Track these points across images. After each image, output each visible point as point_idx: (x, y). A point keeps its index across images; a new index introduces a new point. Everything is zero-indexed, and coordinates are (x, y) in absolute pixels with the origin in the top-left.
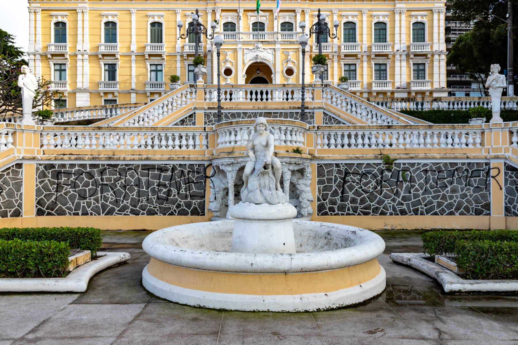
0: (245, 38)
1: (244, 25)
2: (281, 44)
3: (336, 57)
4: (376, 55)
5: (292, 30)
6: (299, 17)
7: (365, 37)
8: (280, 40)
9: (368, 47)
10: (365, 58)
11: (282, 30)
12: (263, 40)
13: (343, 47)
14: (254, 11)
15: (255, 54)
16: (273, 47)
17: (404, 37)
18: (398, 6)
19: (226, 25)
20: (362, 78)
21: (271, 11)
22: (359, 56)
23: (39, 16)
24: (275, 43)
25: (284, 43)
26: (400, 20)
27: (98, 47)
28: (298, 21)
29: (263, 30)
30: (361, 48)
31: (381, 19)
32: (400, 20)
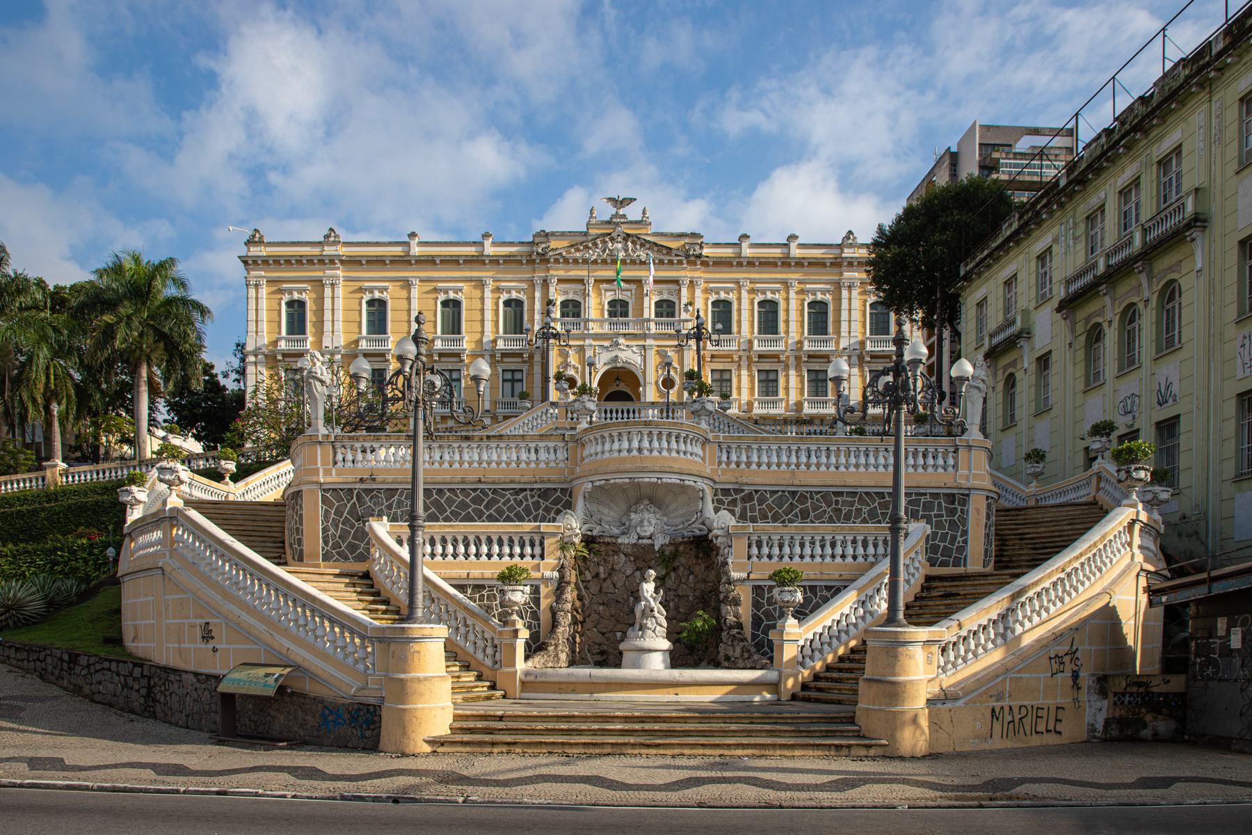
0: (594, 328)
1: (595, 306)
2: (655, 339)
3: (744, 358)
4: (810, 356)
5: (673, 315)
6: (684, 291)
7: (793, 326)
8: (653, 331)
9: (797, 343)
10: (792, 360)
11: (657, 315)
12: (627, 331)
13: (756, 342)
14: (610, 281)
15: (613, 354)
16: (642, 343)
17: (857, 326)
18: (846, 274)
19: (564, 304)
20: (787, 394)
21: (640, 281)
22: (783, 358)
23: (264, 291)
24: (644, 337)
25: (657, 337)
26: (850, 299)
27: (357, 342)
28: (684, 300)
29: (626, 315)
30: (786, 343)
31: (819, 297)
32: (850, 299)
